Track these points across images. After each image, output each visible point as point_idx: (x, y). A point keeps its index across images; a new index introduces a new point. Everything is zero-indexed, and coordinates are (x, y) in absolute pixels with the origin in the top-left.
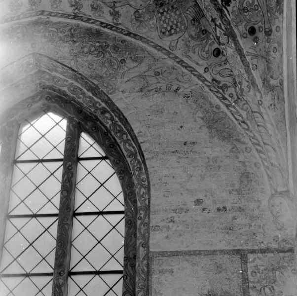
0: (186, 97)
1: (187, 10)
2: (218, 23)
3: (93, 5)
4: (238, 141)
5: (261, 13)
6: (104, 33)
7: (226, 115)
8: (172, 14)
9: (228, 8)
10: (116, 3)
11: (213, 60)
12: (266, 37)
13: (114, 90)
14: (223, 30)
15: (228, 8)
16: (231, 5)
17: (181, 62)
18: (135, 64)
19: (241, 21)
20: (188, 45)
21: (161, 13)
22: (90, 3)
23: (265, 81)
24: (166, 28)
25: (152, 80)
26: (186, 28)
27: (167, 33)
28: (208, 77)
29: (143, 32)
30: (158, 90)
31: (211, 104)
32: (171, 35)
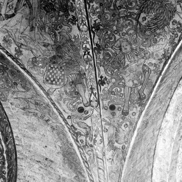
0: (53, 129)
1: (71, 74)
2: (94, 92)
3: (6, 38)
4: (81, 173)
5: (124, 100)
6: (7, 59)
7: (76, 152)
8: (59, 72)
9: (102, 87)
10: (23, 45)
11: (76, 113)
12: (122, 116)
13: (5, 100)
14: (96, 98)
15: (102, 87)
16: (104, 85)
17: (54, 104)
18: (23, 90)
19: (106, 98)
20: (62, 96)
21: (51, 68)
22: (4, 36)
23: (110, 142)
24: (50, 78)
25: (32, 106)
26: (65, 85)
27: (50, 81)
28: (69, 121)
29: (34, 72)
30: (35, 115)
31: (67, 140)
32: (53, 84)
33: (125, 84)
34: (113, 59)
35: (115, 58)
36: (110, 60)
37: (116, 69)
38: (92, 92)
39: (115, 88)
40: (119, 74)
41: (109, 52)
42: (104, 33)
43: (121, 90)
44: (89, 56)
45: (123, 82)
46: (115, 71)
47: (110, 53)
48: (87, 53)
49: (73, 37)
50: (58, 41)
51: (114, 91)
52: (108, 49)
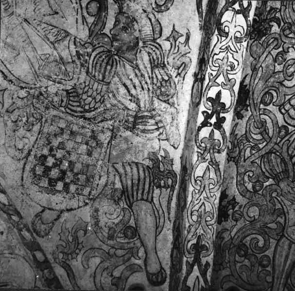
2: (204, 261)
14: (206, 281)
20: (81, 240)
33: (284, 228)
34: (272, 145)
35: (276, 144)
36: (261, 146)
37: (271, 180)
38: (197, 260)
39: (254, 236)
40: (274, 195)
41: (269, 121)
42: (277, 51)
43: (266, 247)
44: (217, 135)
45: (278, 223)
46: (267, 184)
47: (269, 125)
48: (213, 120)
49: (167, 32)
50: (106, 31)
51: (248, 244)
52: (268, 108)
